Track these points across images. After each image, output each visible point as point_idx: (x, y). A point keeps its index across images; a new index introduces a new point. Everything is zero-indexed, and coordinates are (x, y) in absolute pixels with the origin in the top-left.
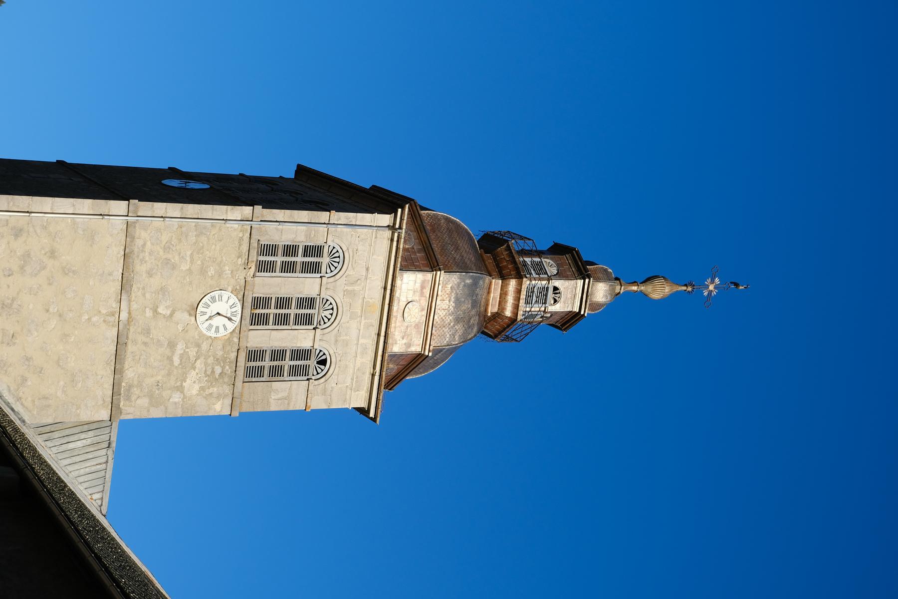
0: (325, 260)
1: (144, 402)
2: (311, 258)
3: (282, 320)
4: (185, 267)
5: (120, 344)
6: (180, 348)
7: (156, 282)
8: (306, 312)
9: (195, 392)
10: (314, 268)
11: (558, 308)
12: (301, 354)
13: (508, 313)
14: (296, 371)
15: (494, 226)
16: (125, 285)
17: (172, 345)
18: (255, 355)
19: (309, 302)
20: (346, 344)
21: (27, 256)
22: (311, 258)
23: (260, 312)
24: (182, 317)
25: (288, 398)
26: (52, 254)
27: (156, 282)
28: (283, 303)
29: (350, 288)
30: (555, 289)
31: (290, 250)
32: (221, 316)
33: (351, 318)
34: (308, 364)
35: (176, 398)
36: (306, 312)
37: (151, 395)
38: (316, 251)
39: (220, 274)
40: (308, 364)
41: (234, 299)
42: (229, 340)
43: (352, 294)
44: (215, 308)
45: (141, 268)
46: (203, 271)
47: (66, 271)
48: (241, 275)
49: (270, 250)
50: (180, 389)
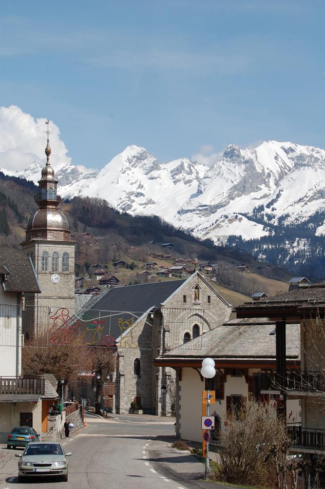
1: (71, 292)
4: (46, 286)
23: (55, 270)
32: (55, 278)
35: (71, 286)
37: (70, 291)
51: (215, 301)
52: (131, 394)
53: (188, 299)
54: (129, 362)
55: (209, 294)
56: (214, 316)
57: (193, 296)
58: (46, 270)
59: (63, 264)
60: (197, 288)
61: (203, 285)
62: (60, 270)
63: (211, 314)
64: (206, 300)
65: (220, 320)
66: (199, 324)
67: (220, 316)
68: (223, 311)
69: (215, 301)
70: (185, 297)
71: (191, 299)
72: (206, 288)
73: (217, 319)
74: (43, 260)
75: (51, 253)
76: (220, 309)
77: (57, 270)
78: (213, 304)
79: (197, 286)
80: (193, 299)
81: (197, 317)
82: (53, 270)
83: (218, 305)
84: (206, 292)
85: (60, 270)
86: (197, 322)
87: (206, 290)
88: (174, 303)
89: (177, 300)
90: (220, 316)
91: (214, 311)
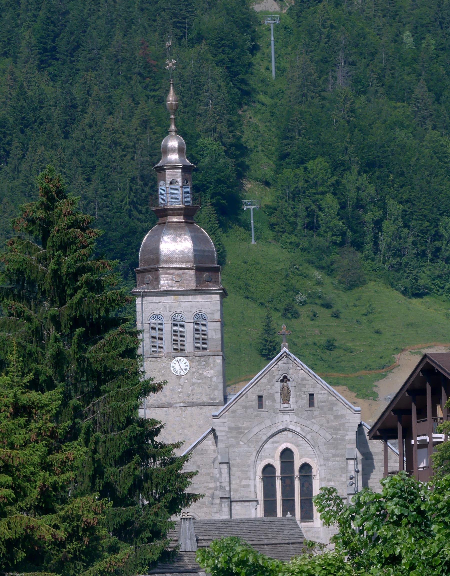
1: (216, 392)
3: (182, 337)
5: (193, 405)
6: (194, 380)
9: (212, 372)
10: (161, 328)
11: (180, 180)
12: (196, 328)
13: (182, 212)
14: (204, 328)
17: (193, 384)
18: (197, 348)
19: (175, 326)
20: (192, 307)
22: (156, 328)
23: (179, 350)
25: (215, 330)
29: (168, 309)
30: (171, 183)
33: (180, 306)
35: (214, 379)
37: (214, 390)
39: (164, 368)
42: (191, 361)
43: (170, 308)
48: (164, 359)
50: (211, 378)
51: (325, 402)
53: (266, 403)
55: (311, 391)
56: (322, 432)
57: (278, 396)
58: (161, 350)
59: (196, 337)
60: (285, 379)
62: (189, 347)
63: (316, 428)
64: (305, 401)
65: (336, 439)
69: (325, 402)
71: (274, 400)
72: (304, 379)
73: (329, 437)
75: (166, 315)
77: (183, 347)
79: (285, 377)
81: (290, 435)
82: (176, 350)
83: (331, 409)
85: (189, 347)
86: (284, 446)
87: (305, 382)
90: (336, 429)
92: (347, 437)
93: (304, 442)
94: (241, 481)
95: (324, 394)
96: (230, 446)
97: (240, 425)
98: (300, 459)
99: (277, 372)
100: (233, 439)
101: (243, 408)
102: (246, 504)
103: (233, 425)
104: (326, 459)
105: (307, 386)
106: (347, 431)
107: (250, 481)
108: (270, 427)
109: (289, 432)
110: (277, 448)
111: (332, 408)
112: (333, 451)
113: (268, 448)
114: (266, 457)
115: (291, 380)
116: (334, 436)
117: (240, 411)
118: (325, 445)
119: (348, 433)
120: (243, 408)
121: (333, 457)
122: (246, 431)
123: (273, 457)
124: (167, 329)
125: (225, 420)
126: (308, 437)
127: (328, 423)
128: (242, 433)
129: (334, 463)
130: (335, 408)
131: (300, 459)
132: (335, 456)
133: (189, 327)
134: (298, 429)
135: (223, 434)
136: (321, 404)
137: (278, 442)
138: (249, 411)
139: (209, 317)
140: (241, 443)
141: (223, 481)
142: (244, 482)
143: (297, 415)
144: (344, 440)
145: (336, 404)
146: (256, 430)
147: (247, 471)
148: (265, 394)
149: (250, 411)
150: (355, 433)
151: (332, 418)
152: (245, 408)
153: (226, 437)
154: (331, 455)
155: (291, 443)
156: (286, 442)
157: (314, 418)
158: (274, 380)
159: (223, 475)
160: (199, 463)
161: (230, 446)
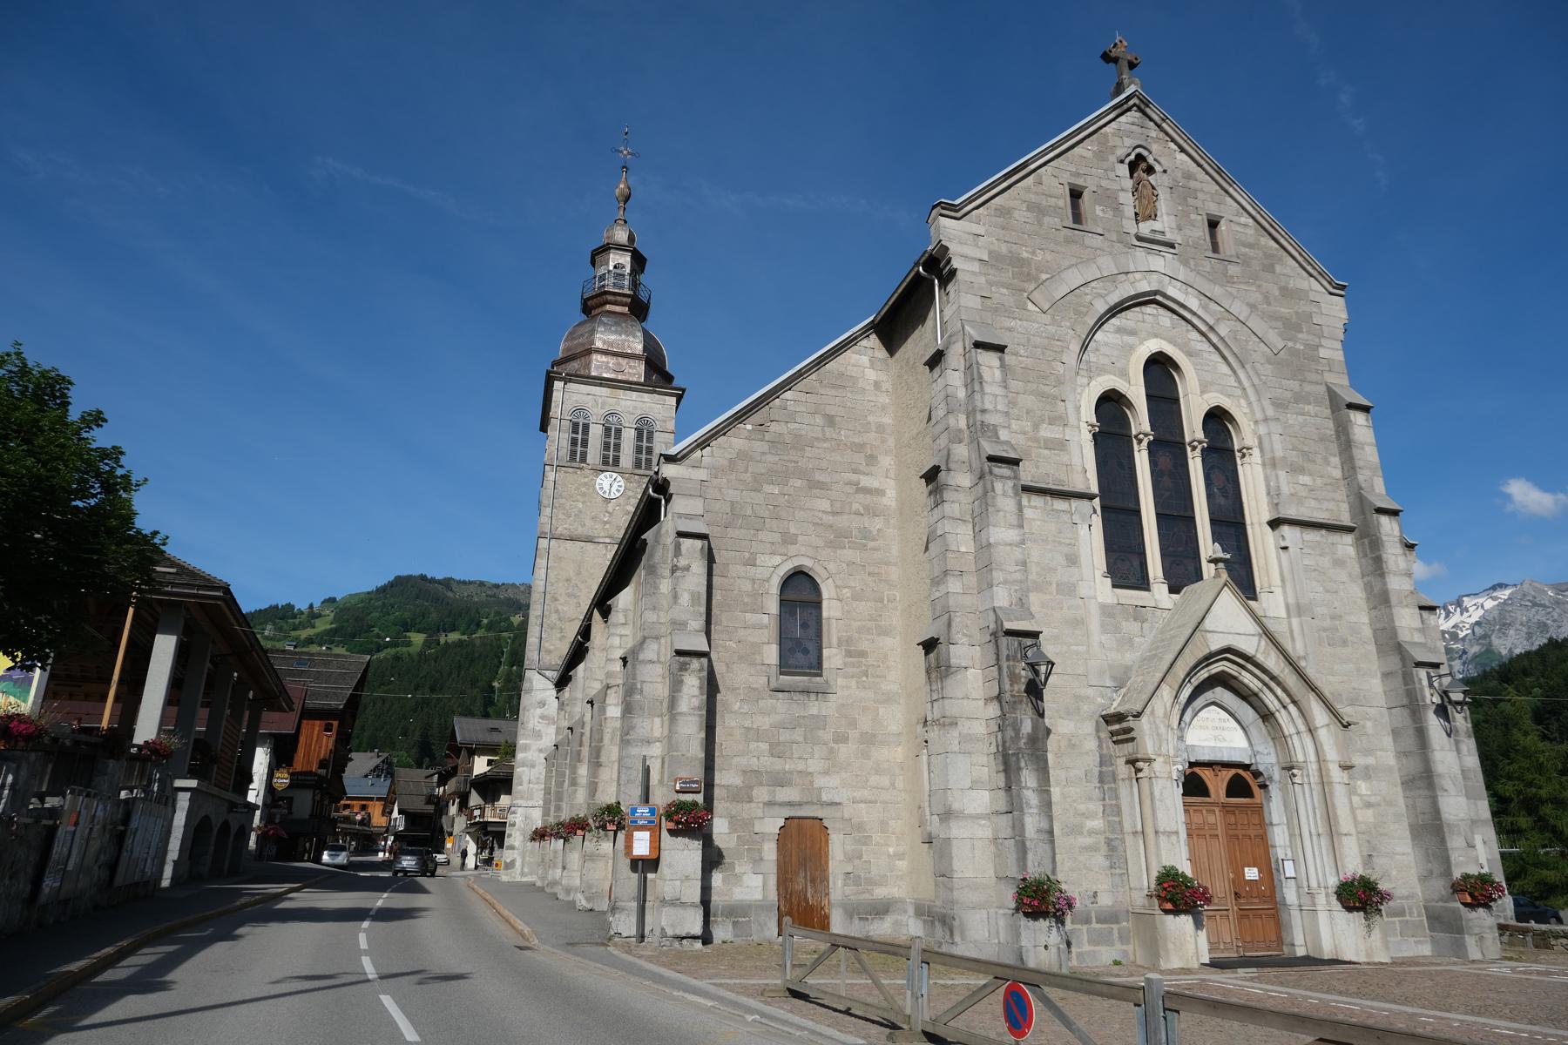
0: (581, 421)
2: (579, 430)
3: (617, 447)
7: (588, 522)
8: (612, 433)
10: (586, 427)
12: (639, 437)
14: (650, 439)
15: (579, 306)
16: (589, 540)
19: (607, 430)
21: (569, 595)
22: (579, 430)
23: (610, 461)
24: (610, 507)
26: (568, 580)
27: (588, 522)
28: (606, 446)
31: (574, 442)
34: (644, 432)
36: (612, 433)
38: (575, 426)
40: (644, 432)
41: (602, 476)
43: (604, 404)
44: (606, 488)
45: (580, 531)
46: (583, 495)
47: (579, 573)
49: (573, 454)
51: (1250, 246)
52: (761, 794)
54: (747, 586)
55: (1214, 209)
58: (583, 459)
61: (1171, 160)
62: (627, 459)
63: (1238, 308)
65: (1294, 353)
66: (1170, 350)
67: (1290, 327)
68: (1304, 307)
69: (1250, 246)
70: (1076, 194)
71: (1117, 208)
72: (1189, 176)
74: (575, 431)
75: (596, 416)
76: (1287, 293)
78: (1245, 261)
79: (1140, 157)
80: (1129, 212)
81: (1166, 318)
82: (605, 463)
83: (1270, 269)
84: (1193, 193)
85: (627, 459)
86: (1153, 346)
87: (1192, 184)
88: (1016, 214)
89: (1032, 198)
91: (1256, 297)
92: (1323, 353)
93: (1206, 346)
94: (1036, 427)
95: (1246, 225)
96: (996, 310)
97: (1025, 255)
98: (1202, 392)
99: (1118, 142)
100: (1004, 291)
101: (1028, 210)
102: (1060, 505)
103: (1004, 249)
104: (1278, 404)
105: (1199, 195)
106: (1322, 336)
107: (1067, 430)
108: (1112, 278)
109: (1162, 311)
110: (1131, 349)
111: (1272, 266)
112: (1294, 385)
113: (1106, 344)
114: (1102, 370)
115: (1157, 168)
116: (1290, 344)
117: (1021, 215)
118: (1269, 362)
119: (1324, 342)
120: (1028, 210)
121: (1296, 402)
122: (1044, 276)
123: (1123, 374)
124: (596, 432)
125: (980, 230)
126: (1223, 330)
127: (1269, 304)
128: (1029, 277)
129: (1301, 418)
130: (1278, 268)
131: (1202, 392)
132: (1299, 398)
133: (629, 436)
134: (1193, 303)
135: (976, 267)
136: (1244, 250)
137: (1133, 333)
138: (1046, 220)
139: (658, 426)
140: (1030, 306)
141: (988, 406)
142: (1047, 432)
143: (1185, 263)
144: (1316, 359)
145: (1280, 259)
146: (1074, 278)
147: (1055, 398)
148: (1089, 185)
149: (1051, 221)
150: (1339, 346)
151: (1277, 293)
152: (1038, 210)
153: (982, 280)
154: (1288, 395)
155: (1171, 341)
156: (1156, 336)
157: (1230, 280)
158: (1112, 159)
159: (988, 389)
160: (831, 411)
161: (996, 310)
